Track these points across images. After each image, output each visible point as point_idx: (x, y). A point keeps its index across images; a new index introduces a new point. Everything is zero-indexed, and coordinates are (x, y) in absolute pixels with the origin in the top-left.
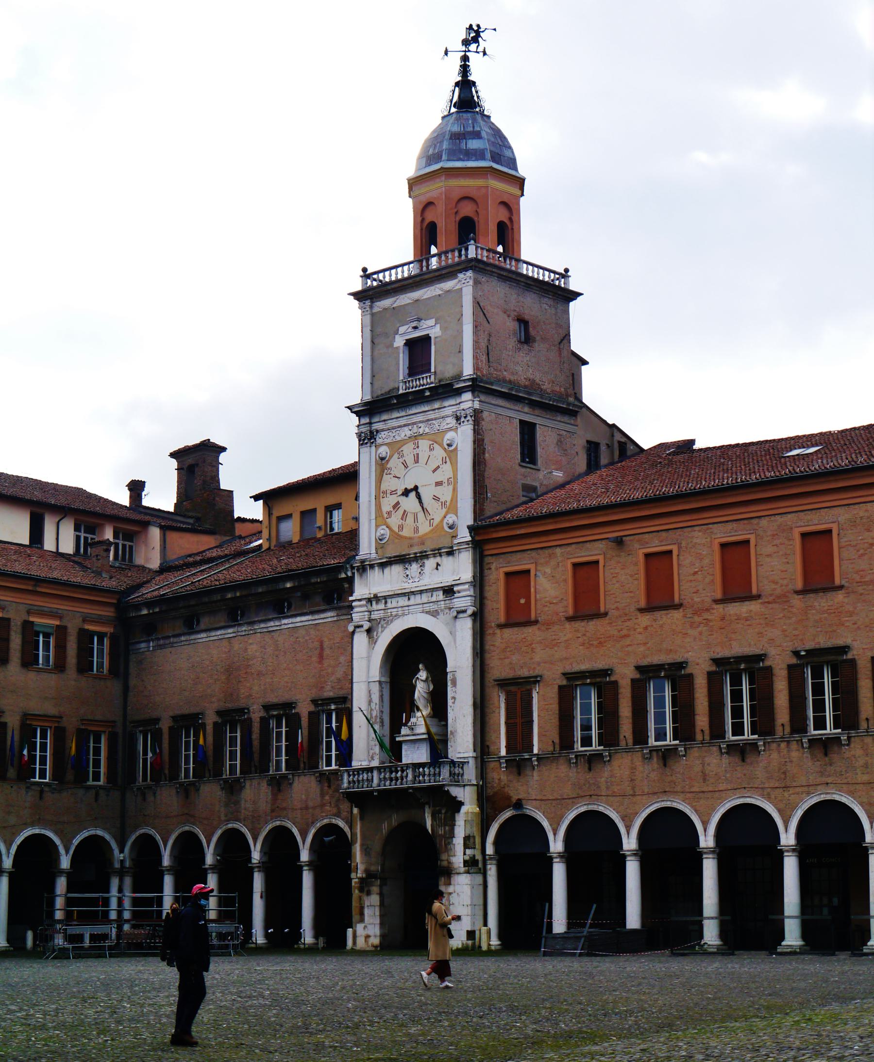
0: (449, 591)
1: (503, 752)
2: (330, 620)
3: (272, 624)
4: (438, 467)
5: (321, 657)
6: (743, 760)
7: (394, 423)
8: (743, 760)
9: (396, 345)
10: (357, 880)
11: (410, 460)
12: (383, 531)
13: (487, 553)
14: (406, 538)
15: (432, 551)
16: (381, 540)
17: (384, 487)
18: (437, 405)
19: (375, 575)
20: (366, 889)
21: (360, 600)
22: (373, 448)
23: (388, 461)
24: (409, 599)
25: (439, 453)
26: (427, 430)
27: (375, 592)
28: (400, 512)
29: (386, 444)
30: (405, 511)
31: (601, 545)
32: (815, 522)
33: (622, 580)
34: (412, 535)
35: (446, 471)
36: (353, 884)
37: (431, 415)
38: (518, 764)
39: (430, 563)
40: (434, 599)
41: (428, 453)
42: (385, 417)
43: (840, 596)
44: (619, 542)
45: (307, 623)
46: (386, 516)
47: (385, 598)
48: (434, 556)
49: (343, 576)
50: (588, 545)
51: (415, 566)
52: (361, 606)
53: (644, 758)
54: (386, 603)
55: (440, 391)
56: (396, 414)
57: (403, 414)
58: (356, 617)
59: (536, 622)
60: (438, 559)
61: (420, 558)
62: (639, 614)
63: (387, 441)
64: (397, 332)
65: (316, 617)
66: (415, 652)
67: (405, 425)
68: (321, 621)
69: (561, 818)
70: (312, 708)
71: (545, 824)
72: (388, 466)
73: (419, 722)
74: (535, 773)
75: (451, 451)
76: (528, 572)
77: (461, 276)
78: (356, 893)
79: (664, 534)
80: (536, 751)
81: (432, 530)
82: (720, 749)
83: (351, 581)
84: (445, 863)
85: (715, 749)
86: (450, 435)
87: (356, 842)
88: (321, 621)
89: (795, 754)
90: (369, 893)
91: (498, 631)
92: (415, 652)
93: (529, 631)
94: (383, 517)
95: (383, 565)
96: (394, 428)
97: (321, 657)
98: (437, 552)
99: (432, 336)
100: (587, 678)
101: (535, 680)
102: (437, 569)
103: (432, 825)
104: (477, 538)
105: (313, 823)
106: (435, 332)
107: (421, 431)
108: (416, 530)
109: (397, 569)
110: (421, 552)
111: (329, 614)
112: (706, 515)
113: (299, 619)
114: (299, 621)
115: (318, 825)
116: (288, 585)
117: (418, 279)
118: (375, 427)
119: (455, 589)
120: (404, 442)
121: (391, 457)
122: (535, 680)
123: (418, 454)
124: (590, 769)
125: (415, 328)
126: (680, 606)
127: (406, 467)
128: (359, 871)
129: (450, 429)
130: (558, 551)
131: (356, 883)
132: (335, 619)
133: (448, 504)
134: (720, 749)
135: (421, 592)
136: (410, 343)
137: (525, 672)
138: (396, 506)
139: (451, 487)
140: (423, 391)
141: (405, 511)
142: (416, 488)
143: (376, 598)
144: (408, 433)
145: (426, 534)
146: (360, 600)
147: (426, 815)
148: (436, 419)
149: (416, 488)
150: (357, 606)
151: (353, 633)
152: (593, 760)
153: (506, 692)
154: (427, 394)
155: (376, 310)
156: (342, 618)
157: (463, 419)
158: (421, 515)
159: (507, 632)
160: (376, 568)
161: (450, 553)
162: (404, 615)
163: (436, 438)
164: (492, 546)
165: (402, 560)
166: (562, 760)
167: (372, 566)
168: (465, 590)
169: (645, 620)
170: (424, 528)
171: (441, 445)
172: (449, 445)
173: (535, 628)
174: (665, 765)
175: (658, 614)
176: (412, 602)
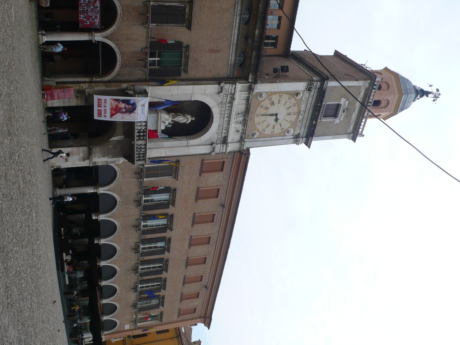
0: (225, 141)
1: (145, 166)
2: (230, 58)
3: (239, 8)
4: (281, 126)
5: (212, 51)
6: (133, 249)
7: (310, 101)
8: (133, 249)
9: (343, 99)
10: (84, 88)
11: (290, 111)
12: (264, 96)
13: (236, 154)
14: (256, 109)
15: (246, 130)
16: (260, 96)
17: (284, 95)
18: (307, 124)
19: (245, 95)
20: (78, 95)
21: (235, 88)
22: (303, 89)
23: (294, 98)
24: (227, 117)
25: (286, 125)
26: (299, 120)
27: (236, 99)
28: (269, 106)
29: (302, 97)
30: (268, 108)
31: (224, 198)
32: (209, 261)
33: (208, 206)
34: (257, 113)
35: (278, 130)
36: (82, 85)
37: (304, 122)
38: (140, 174)
39: (240, 127)
40: (224, 131)
41: (289, 120)
42: (315, 95)
43: (184, 267)
44: (223, 206)
45: (232, 39)
46: (270, 97)
47: (231, 103)
48: (243, 130)
49: (250, 76)
50: (225, 193)
51: (241, 119)
52: (232, 90)
53: (137, 220)
54: (229, 103)
55: (312, 129)
56: (314, 101)
57: (312, 106)
58: (227, 87)
59: (200, 175)
60: (241, 131)
61: (245, 123)
62: (193, 213)
63: (304, 97)
64: (347, 100)
65: (234, 47)
66: (201, 118)
67: (306, 107)
68: (231, 50)
69: (114, 192)
70: (185, 45)
71: (112, 185)
72: (292, 98)
73: (166, 120)
74: (135, 180)
75: (285, 133)
76: (222, 170)
77: (352, 135)
78: (77, 87)
79: (220, 219)
80: (145, 179)
81: (255, 124)
82: (138, 242)
83: (246, 79)
84: (94, 150)
85: (138, 241)
86: (292, 133)
87: (106, 87)
88: (231, 50)
89: (133, 262)
90: (77, 97)
91: (201, 160)
92: (201, 118)
93: (198, 172)
94: (270, 96)
95: (248, 99)
96: (308, 102)
97: (212, 51)
98: (244, 133)
99: (336, 119)
100: (173, 197)
101: (176, 177)
102: (237, 131)
103: (114, 140)
104: (243, 156)
105: (117, 45)
106: (337, 121)
107: (300, 117)
108: (258, 116)
109: (242, 107)
110: (247, 124)
111: (233, 58)
112: (222, 232)
113: (236, 32)
114: (236, 32)
115: (116, 50)
116: (257, 32)
117: (362, 114)
118: (313, 91)
119: (225, 146)
120: (299, 106)
121: (296, 100)
122: (176, 177)
123: (291, 115)
124: (134, 201)
125: (344, 111)
126: (193, 225)
127: (288, 108)
128: (89, 89)
129: (294, 132)
130: (227, 182)
131: (82, 87)
132: (230, 63)
133: (264, 132)
134: (138, 242)
135: (229, 124)
136: (338, 106)
137: (180, 172)
138: (273, 103)
139: (270, 133)
140: (316, 121)
141: (268, 108)
142: (276, 115)
143: (233, 99)
144: (302, 110)
145: (254, 121)
146: (235, 88)
147: (119, 137)
148: (302, 124)
149: (276, 115)
150: (232, 86)
151: (219, 84)
152: (138, 202)
153: (172, 167)
154: (314, 122)
155: (362, 88)
156: (229, 67)
157: (296, 140)
158: (264, 112)
159: (199, 164)
160: (247, 95)
161: (242, 140)
162: (221, 114)
163: (294, 125)
164: (238, 156)
165: (247, 111)
166: (140, 190)
167: (249, 93)
168: (223, 150)
169: (191, 215)
170: (257, 120)
171: (289, 128)
172: (288, 132)
173: (198, 175)
174: (133, 226)
175: (191, 220)
176: (226, 119)
